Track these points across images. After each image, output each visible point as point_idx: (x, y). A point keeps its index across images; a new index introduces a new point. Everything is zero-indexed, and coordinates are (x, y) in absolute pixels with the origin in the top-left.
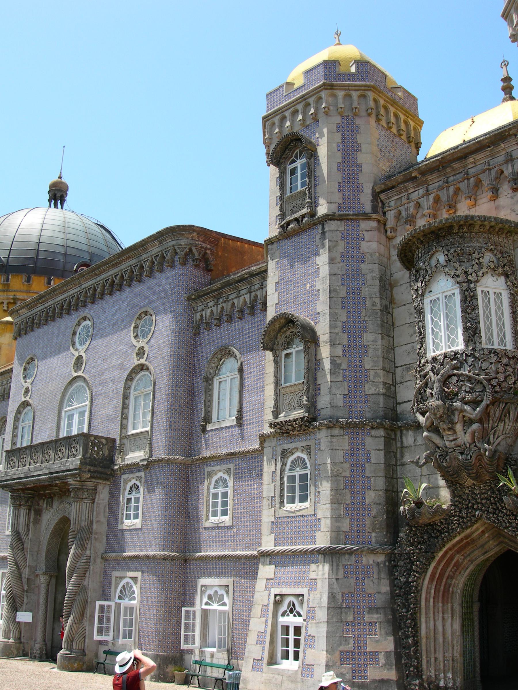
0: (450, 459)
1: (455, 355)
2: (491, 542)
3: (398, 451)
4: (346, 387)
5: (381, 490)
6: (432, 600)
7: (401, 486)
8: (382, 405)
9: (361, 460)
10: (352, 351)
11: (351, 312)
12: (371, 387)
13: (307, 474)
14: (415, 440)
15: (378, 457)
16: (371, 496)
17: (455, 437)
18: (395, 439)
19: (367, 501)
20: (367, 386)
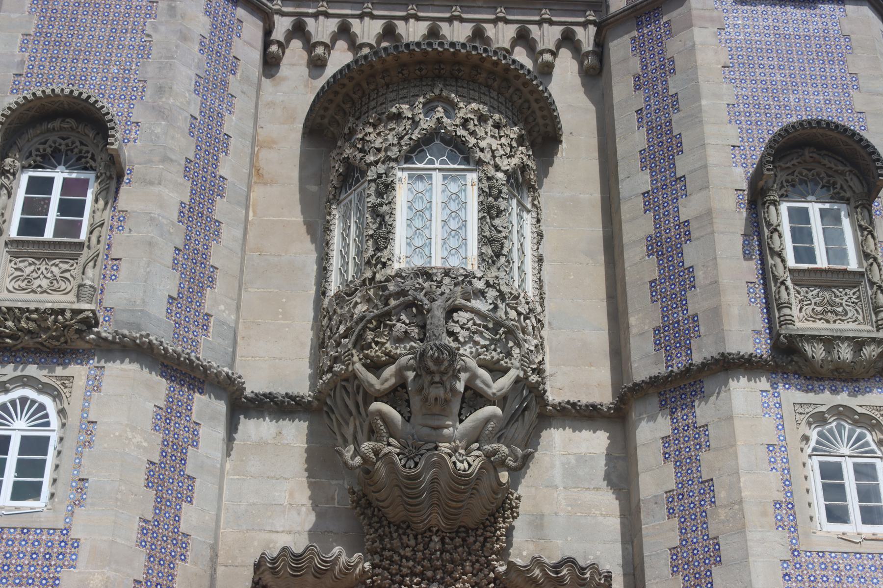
1: (466, 276)
10: (195, 221)
11: (203, 150)
13: (47, 439)
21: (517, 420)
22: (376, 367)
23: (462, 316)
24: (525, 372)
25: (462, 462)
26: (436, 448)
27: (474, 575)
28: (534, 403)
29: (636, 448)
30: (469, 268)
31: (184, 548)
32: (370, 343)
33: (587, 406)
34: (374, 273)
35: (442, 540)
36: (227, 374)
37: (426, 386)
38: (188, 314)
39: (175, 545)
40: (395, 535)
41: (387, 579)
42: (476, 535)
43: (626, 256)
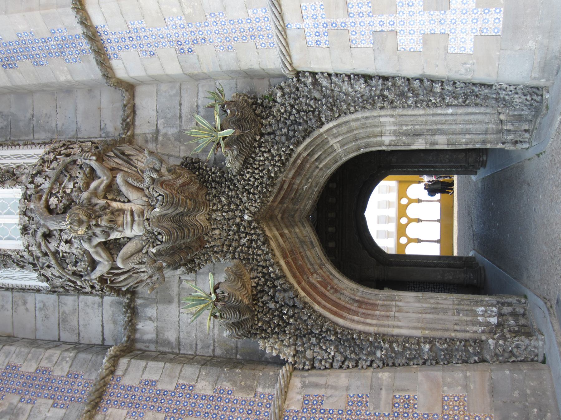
0: (158, 227)
1: (26, 199)
2: (297, 230)
3: (161, 349)
4: (43, 401)
5: (200, 371)
6: (368, 321)
7: (207, 350)
8: (90, 356)
9: (149, 395)
12: (60, 367)
14: (150, 319)
15: (154, 371)
16: (204, 387)
17: (129, 213)
18: (145, 351)
19: (209, 393)
20: (57, 373)
21: (132, 160)
22: (93, 264)
23: (53, 201)
24: (95, 155)
25: (157, 200)
26: (148, 219)
27: (238, 188)
28: (118, 148)
29: (149, 76)
30: (20, 196)
31: (224, 392)
32: (76, 266)
33: (124, 111)
34: (29, 263)
35: (215, 211)
36: (107, 361)
37: (101, 229)
38: (66, 390)
39: (221, 400)
40: (212, 244)
41: (242, 249)
42: (211, 187)
43: (20, 84)
